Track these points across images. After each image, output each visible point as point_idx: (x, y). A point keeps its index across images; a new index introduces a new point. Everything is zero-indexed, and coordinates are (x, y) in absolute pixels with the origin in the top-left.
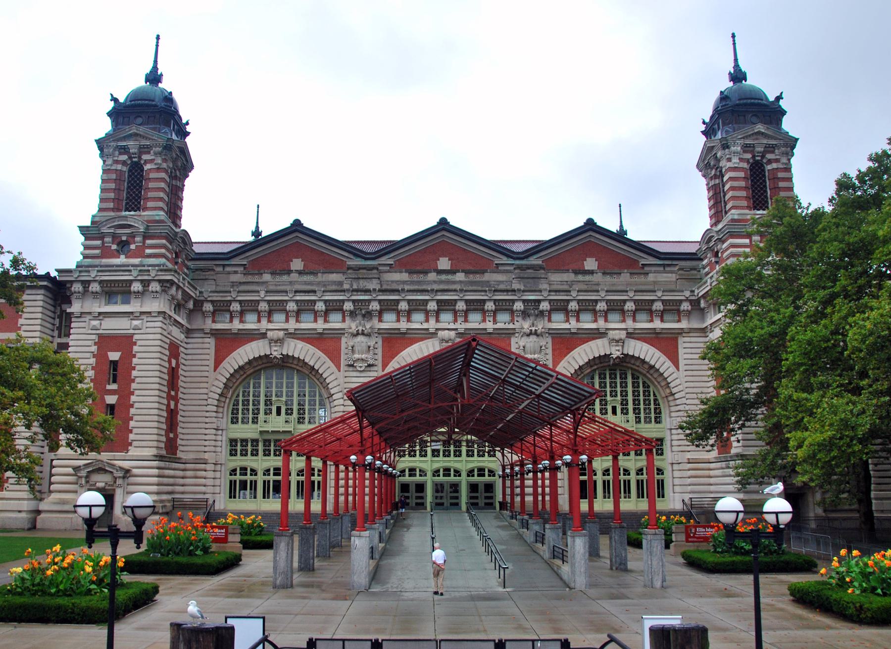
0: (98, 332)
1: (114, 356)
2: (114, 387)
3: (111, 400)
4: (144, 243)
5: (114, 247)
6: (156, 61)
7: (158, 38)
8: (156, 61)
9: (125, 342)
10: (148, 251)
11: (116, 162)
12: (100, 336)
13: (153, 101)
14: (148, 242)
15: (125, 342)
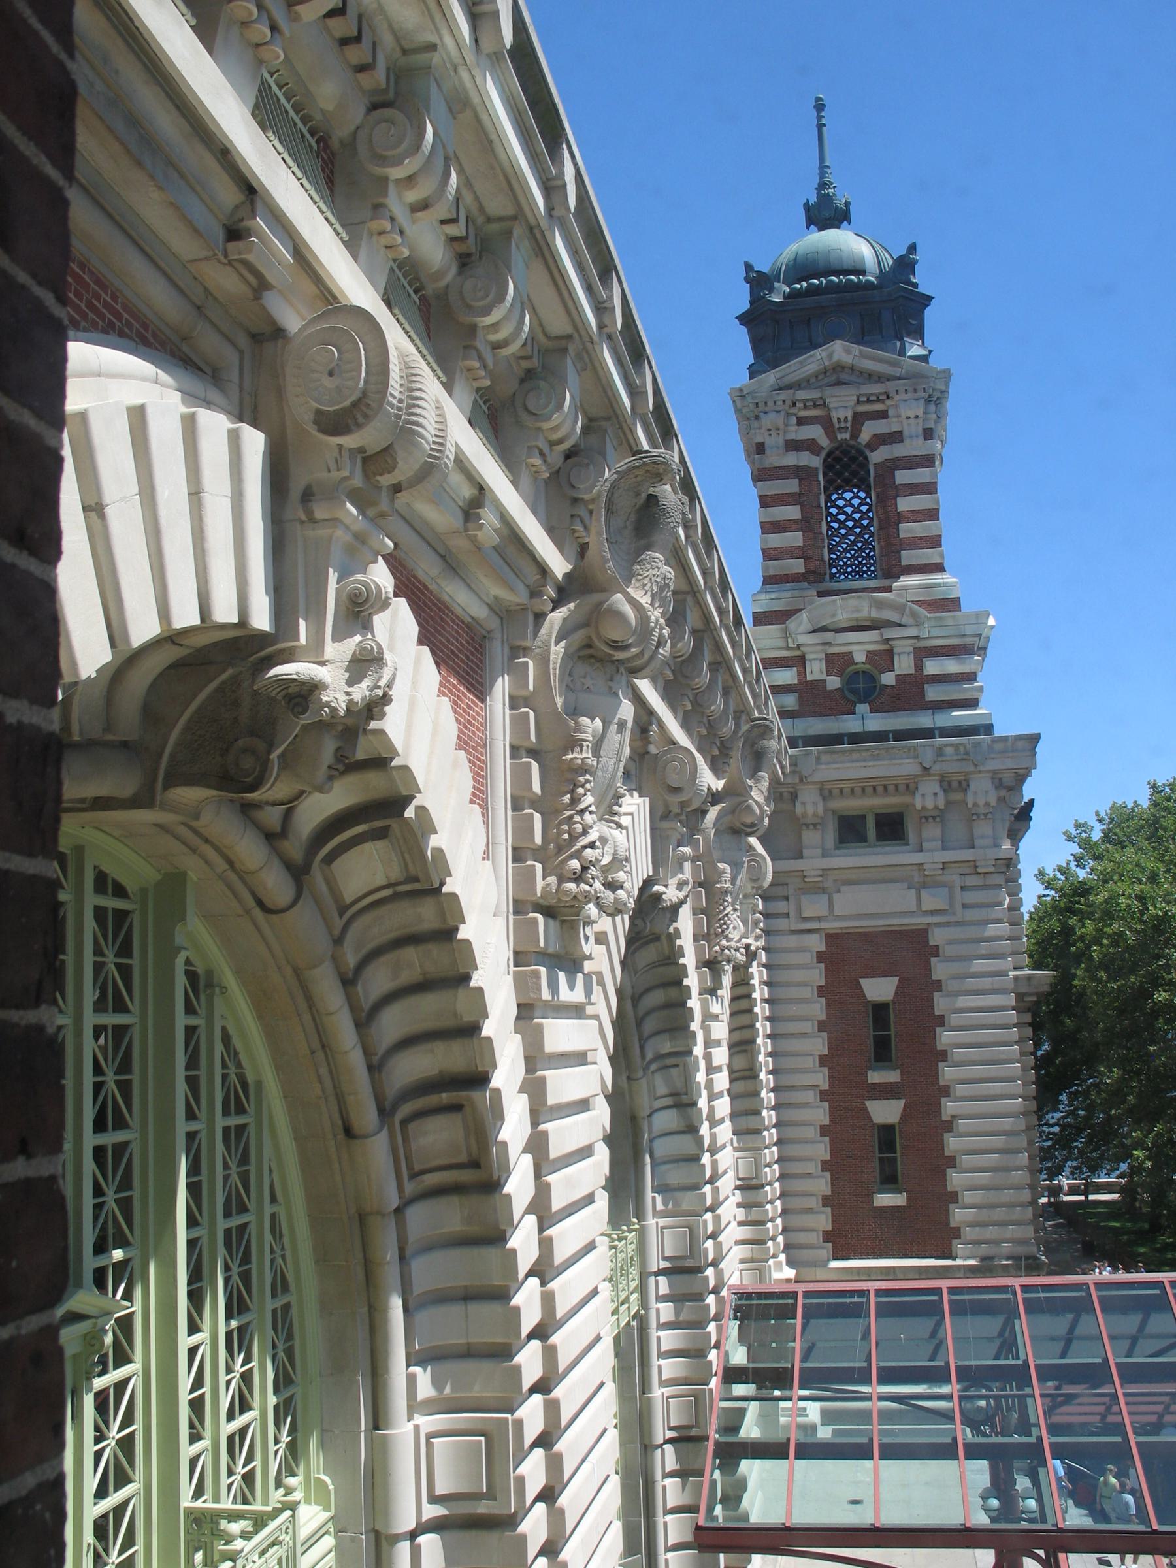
0: (823, 925)
1: (879, 989)
2: (893, 1076)
3: (885, 1112)
4: (919, 667)
5: (834, 682)
6: (823, 168)
7: (820, 106)
8: (823, 168)
9: (909, 951)
10: (933, 693)
11: (793, 446)
12: (832, 938)
13: (863, 273)
14: (932, 667)
15: (909, 951)
